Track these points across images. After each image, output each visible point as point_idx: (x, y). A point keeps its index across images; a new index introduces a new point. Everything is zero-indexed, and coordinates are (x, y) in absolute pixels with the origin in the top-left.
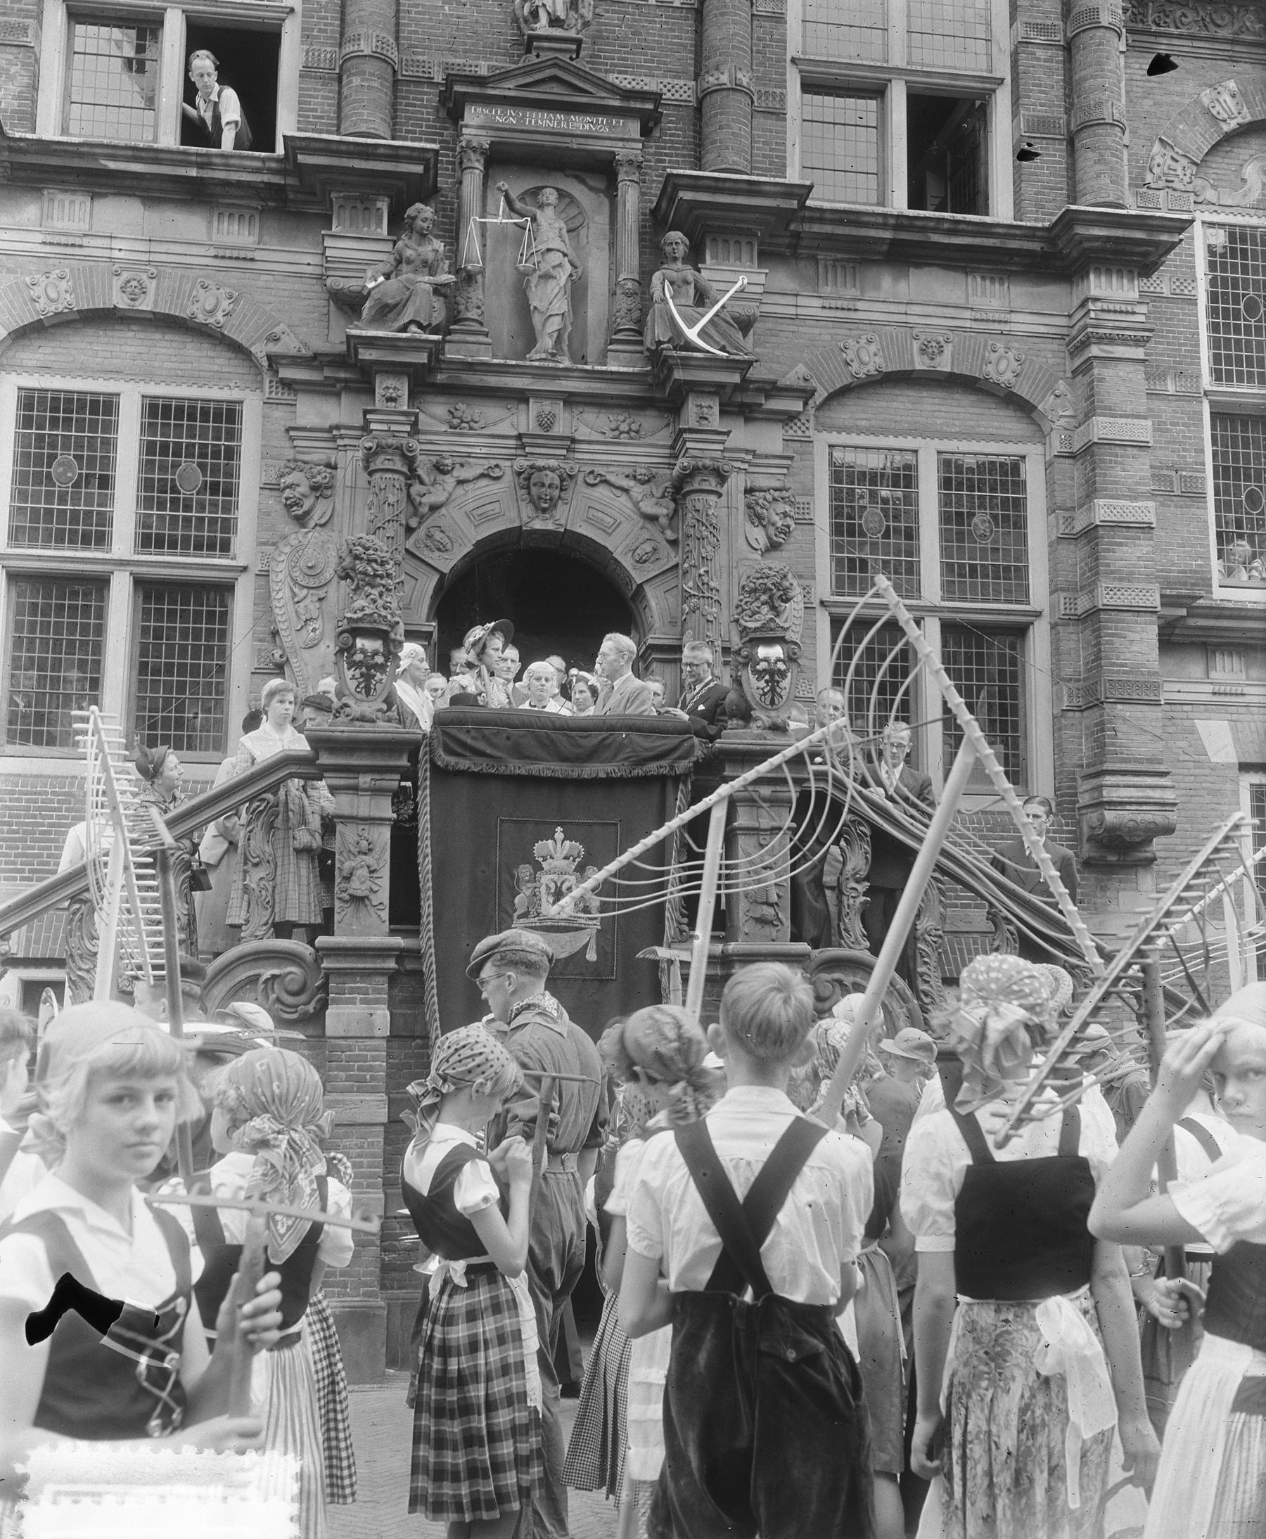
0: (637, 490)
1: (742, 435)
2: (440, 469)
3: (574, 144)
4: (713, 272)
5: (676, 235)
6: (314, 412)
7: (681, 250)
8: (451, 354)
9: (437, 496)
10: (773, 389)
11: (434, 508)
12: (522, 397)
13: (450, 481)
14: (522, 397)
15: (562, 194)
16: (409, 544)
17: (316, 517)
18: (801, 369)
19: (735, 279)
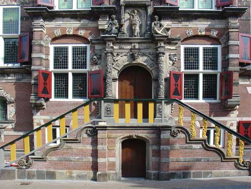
0: (150, 56)
1: (168, 47)
2: (118, 55)
3: (139, 3)
4: (163, 22)
5: (156, 16)
6: (97, 47)
7: (157, 19)
8: (119, 37)
9: (118, 58)
10: (173, 40)
11: (117, 61)
12: (131, 43)
13: (120, 56)
14: (131, 43)
15: (137, 11)
16: (113, 66)
17: (99, 63)
18: (179, 35)
19: (166, 23)
